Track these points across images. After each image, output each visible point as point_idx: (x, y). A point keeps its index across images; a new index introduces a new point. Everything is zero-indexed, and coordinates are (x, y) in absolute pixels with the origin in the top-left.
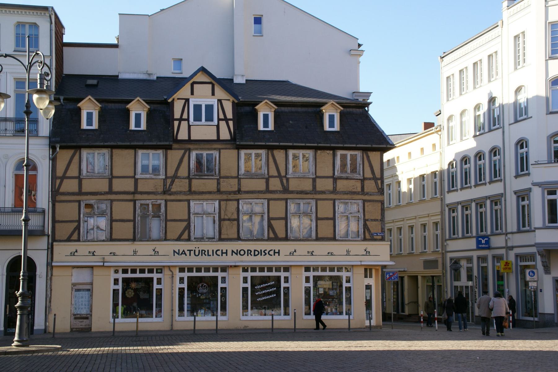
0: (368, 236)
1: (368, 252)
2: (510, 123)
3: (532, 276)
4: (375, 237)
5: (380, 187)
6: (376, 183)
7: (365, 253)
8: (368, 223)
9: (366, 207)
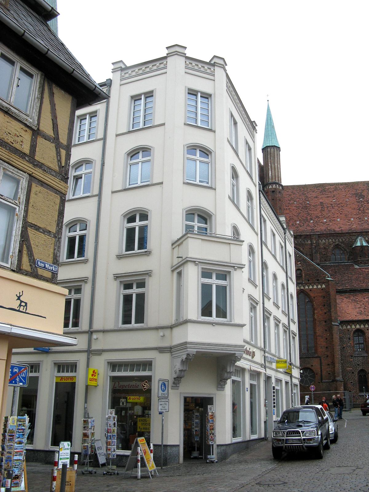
0: (26, 265)
1: (23, 304)
2: (115, 190)
3: (163, 391)
4: (40, 272)
5: (63, 165)
6: (58, 154)
7: (15, 304)
8: (31, 232)
9: (32, 195)
